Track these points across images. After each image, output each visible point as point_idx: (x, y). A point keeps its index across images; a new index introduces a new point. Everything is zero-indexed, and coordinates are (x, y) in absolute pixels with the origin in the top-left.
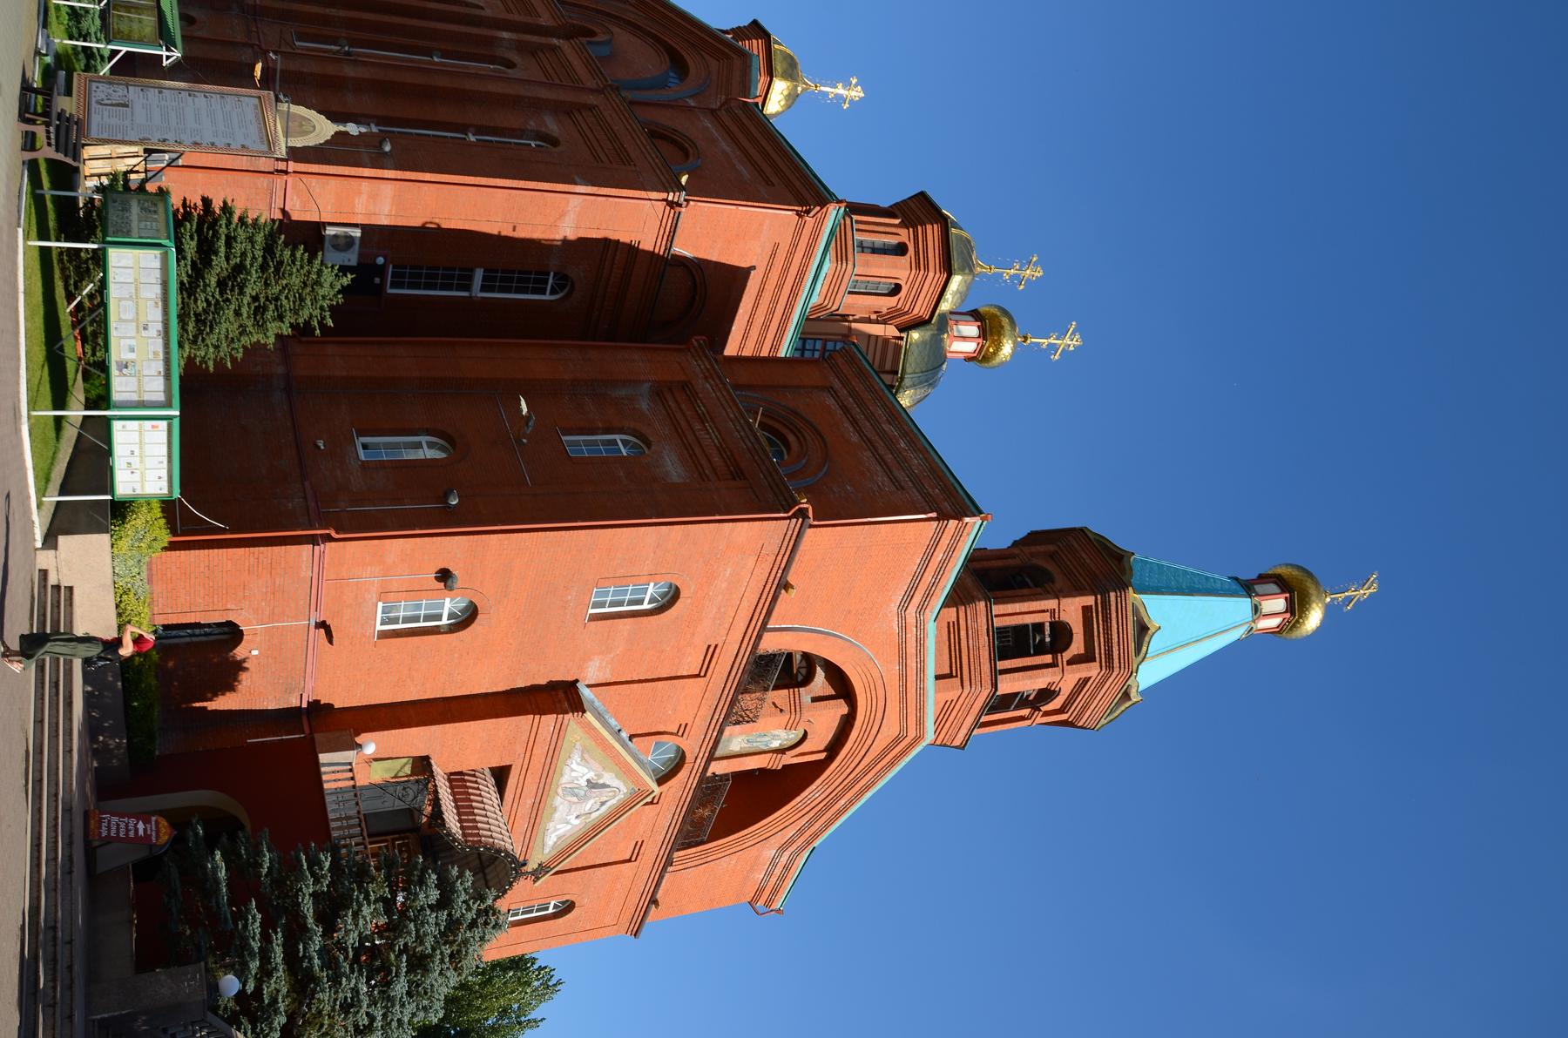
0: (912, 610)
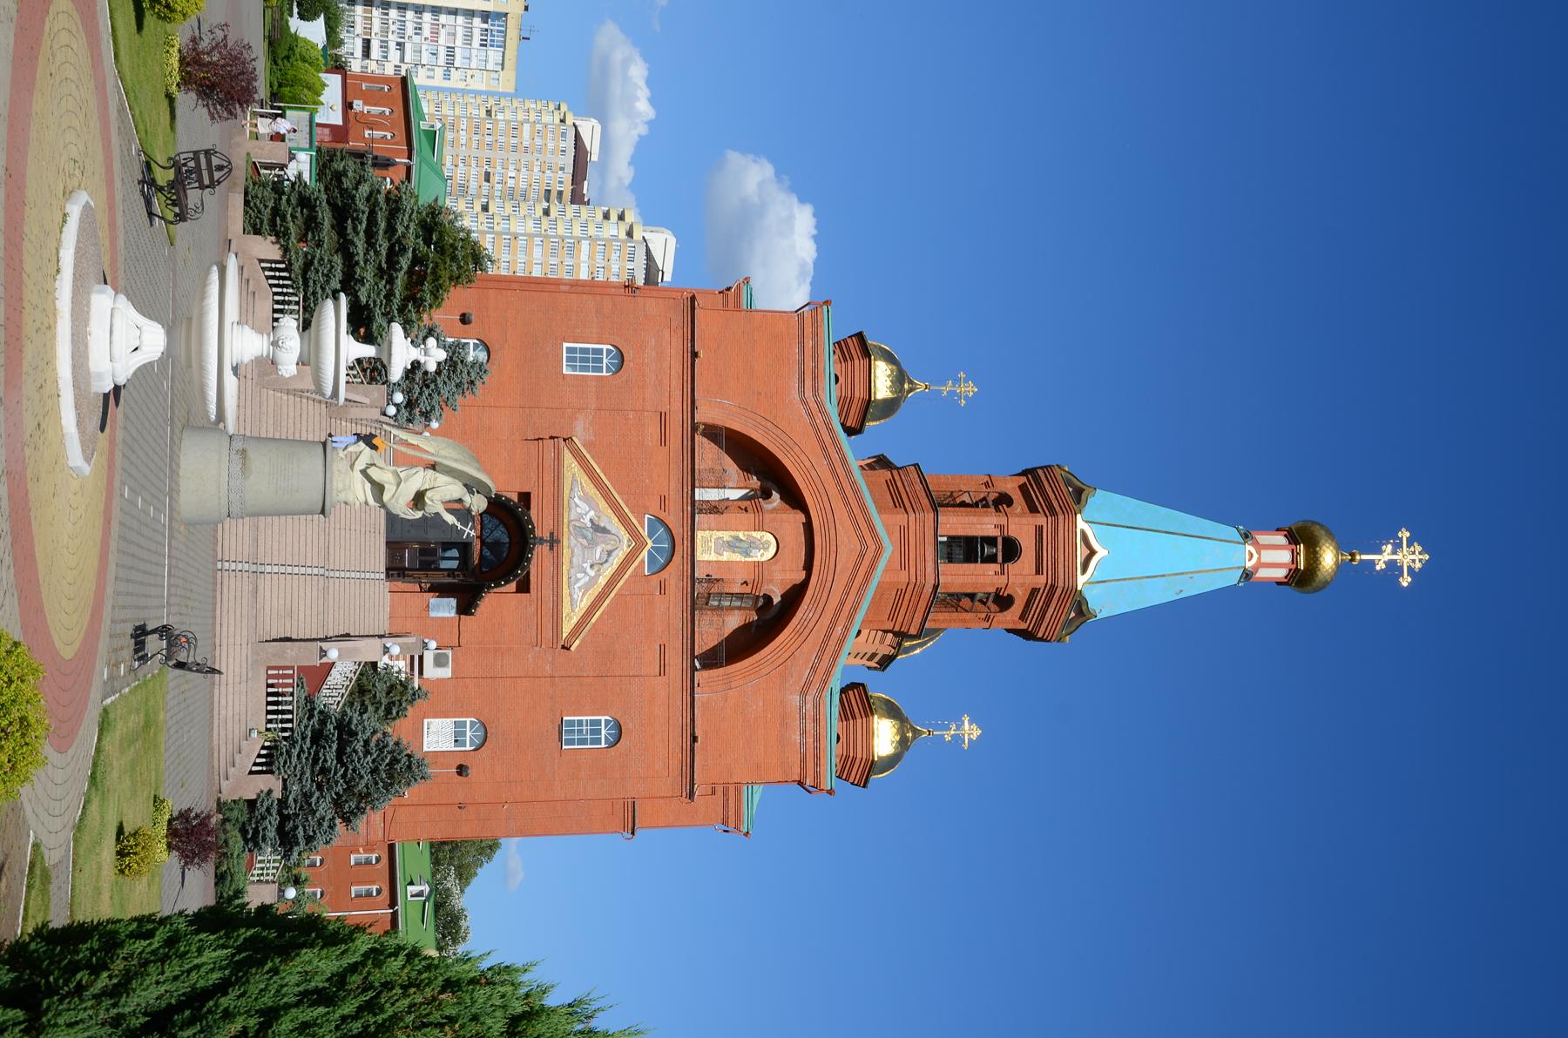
0: (809, 393)
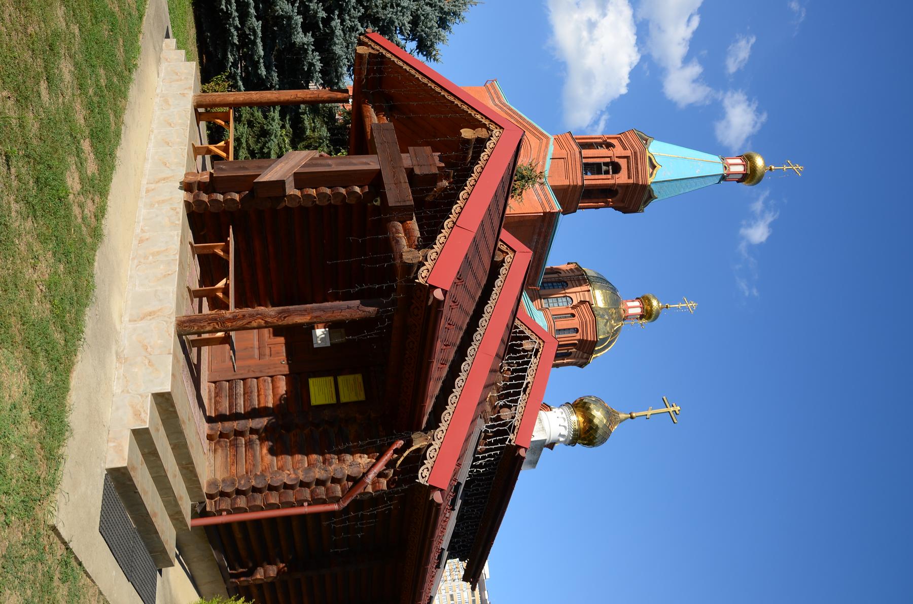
0: (498, 102)
